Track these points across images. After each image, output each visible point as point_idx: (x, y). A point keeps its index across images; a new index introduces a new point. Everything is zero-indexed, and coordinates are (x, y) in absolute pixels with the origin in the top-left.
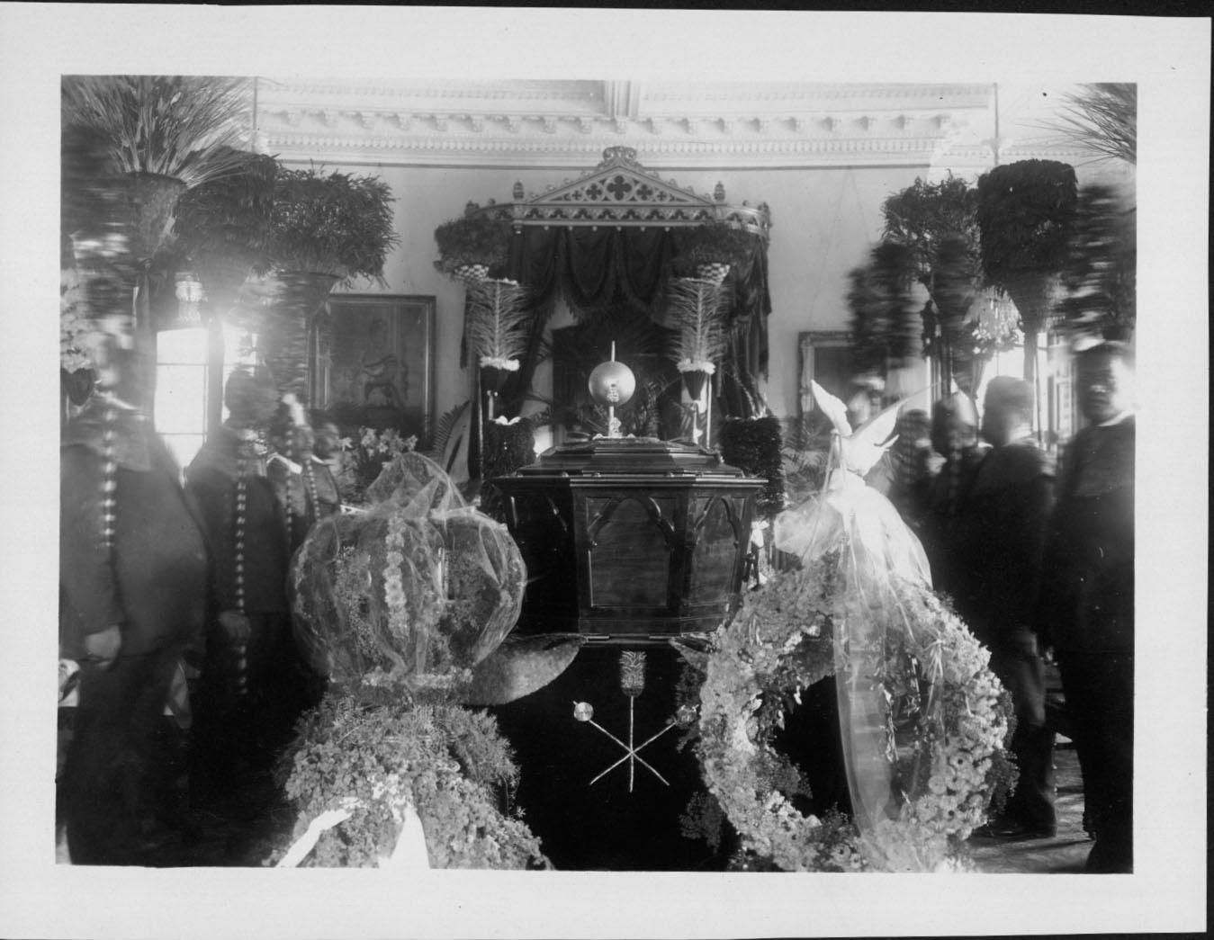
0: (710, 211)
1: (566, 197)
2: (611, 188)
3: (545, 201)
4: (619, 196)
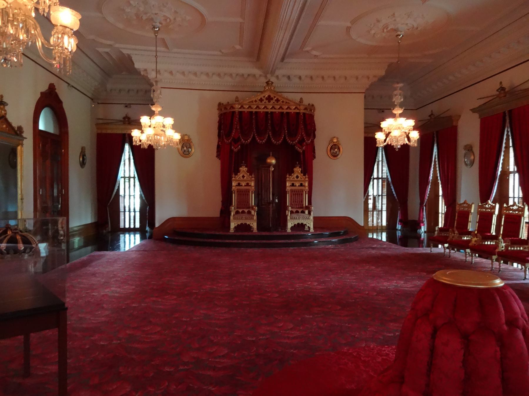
0: (298, 107)
1: (252, 102)
2: (267, 99)
3: (245, 103)
4: (269, 102)
